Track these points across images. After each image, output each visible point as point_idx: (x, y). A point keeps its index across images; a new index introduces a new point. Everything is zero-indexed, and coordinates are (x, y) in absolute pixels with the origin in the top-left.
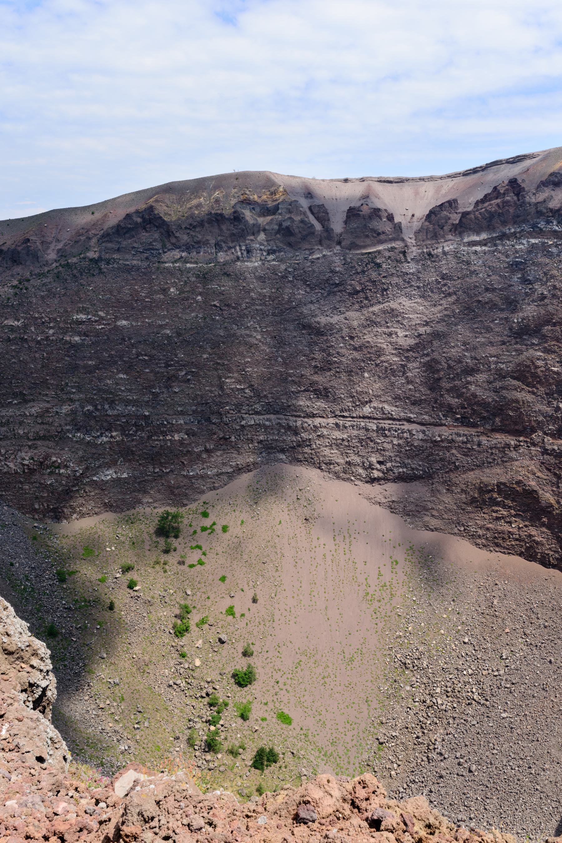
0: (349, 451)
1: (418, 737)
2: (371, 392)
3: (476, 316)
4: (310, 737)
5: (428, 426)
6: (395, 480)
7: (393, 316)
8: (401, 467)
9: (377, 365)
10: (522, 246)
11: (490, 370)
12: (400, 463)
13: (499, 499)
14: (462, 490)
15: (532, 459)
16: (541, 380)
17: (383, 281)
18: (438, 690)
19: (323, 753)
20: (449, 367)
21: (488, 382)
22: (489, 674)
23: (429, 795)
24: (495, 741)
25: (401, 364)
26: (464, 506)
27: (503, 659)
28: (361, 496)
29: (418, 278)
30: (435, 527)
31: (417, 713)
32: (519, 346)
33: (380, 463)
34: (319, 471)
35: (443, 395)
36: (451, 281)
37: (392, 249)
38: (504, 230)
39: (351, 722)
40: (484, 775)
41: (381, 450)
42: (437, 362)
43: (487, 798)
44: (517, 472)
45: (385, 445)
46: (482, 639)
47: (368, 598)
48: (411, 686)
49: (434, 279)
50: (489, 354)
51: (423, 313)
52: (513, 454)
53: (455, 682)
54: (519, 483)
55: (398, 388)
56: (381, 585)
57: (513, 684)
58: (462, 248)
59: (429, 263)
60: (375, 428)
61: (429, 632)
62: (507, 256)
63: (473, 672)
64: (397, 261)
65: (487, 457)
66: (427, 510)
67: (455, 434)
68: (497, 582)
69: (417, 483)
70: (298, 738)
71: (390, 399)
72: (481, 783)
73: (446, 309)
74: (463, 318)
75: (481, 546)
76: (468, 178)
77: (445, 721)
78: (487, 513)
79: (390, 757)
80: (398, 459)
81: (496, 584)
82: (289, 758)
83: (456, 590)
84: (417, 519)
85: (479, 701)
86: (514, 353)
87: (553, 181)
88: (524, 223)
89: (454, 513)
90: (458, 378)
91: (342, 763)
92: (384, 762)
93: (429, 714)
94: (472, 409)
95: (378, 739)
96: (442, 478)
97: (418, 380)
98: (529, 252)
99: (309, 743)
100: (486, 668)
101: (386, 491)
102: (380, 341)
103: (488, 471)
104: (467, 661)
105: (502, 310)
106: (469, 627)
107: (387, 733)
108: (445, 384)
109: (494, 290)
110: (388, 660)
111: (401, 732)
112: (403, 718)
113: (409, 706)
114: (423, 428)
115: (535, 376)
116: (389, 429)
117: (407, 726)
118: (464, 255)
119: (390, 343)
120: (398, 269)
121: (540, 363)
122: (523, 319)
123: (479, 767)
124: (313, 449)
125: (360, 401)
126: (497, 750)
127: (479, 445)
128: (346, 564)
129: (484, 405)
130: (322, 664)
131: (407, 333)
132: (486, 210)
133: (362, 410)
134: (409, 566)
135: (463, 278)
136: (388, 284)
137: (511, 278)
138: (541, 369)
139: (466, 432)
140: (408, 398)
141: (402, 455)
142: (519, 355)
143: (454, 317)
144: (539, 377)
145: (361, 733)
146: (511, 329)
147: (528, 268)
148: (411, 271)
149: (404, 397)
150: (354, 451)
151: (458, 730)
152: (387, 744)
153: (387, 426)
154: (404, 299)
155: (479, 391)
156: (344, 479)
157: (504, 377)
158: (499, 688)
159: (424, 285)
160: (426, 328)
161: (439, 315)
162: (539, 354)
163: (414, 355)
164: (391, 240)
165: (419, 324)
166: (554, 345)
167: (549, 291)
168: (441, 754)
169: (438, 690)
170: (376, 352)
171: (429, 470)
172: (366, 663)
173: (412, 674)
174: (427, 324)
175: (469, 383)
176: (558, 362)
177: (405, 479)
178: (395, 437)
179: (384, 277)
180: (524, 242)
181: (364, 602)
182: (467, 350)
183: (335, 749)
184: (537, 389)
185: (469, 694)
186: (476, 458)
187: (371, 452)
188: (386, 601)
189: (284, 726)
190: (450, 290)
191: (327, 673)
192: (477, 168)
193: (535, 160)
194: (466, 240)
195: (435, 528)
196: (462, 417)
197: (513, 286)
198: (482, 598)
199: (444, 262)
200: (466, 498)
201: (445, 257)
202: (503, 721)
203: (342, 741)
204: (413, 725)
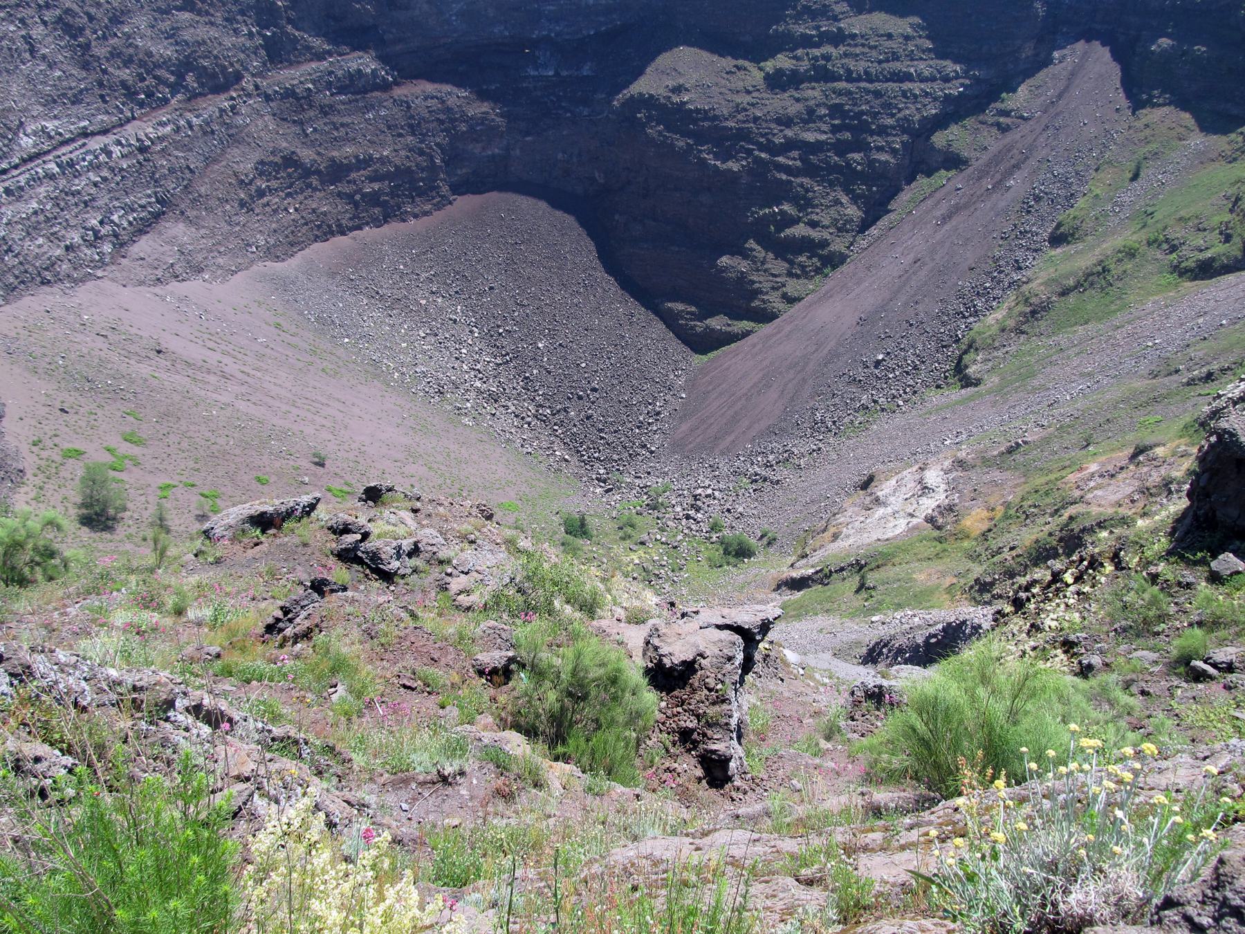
0: (55, 229)
5: (115, 131)
8: (126, 213)
12: (123, 209)
13: (263, 186)
15: (262, 116)
25: (23, 37)
28: (129, 288)
33: (101, 222)
34: (46, 288)
52: (239, 121)
60: (58, 169)
66: (212, 251)
80: (117, 204)
94: (155, 77)
108: (100, 51)
124: (19, 254)
125: (10, 129)
129: (166, 63)
133: (20, 145)
140: (64, 95)
149: (58, 96)
150: (60, 224)
153: (72, 156)
156: (82, 280)
178: (88, 171)
184: (212, 15)
186: (200, 147)
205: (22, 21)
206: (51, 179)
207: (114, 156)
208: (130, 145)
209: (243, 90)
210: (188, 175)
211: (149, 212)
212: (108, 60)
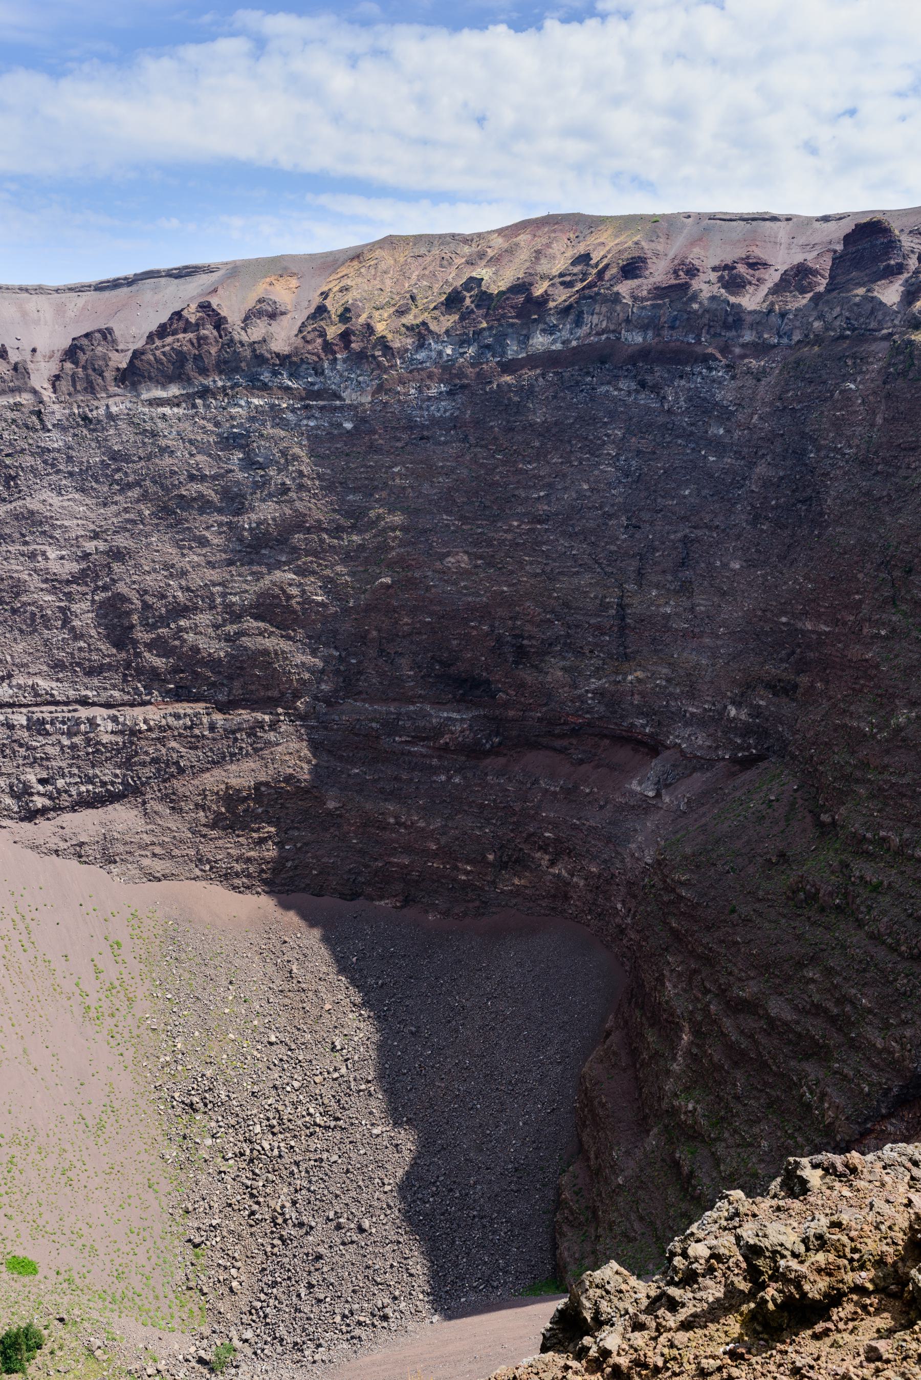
1: (253, 1213)
2: (9, 658)
3: (179, 522)
4: (78, 1281)
5: (120, 708)
6: (73, 807)
7: (34, 524)
8: (82, 783)
9: (14, 611)
10: (240, 410)
11: (215, 607)
12: (80, 777)
14: (197, 805)
15: (302, 740)
16: (299, 616)
17: (7, 462)
18: (258, 1129)
19: (109, 1299)
20: (146, 606)
21: (213, 626)
22: (324, 1079)
23: (310, 1293)
24: (381, 1173)
25: (59, 607)
26: (205, 830)
27: (338, 1051)
29: (68, 457)
30: (162, 873)
31: (238, 1176)
32: (255, 568)
33: (42, 781)
35: (141, 653)
36: (127, 463)
37: (17, 407)
38: (206, 382)
39: (136, 1231)
40: (387, 1227)
41: (42, 758)
42: (124, 599)
43: (406, 1259)
44: (283, 762)
45: (50, 750)
46: (295, 1030)
47: (91, 1015)
48: (213, 1137)
49: (97, 459)
50: (210, 581)
51: (87, 518)
52: (272, 736)
53: (280, 1108)
54: (289, 779)
55: (58, 649)
56: (105, 987)
57: (369, 1082)
58: (141, 409)
59: (85, 432)
60: (25, 723)
61: (211, 1043)
62: (217, 424)
63: (300, 1084)
64: (28, 428)
65: (229, 746)
67: (171, 715)
68: (287, 939)
69: (117, 806)
70: (59, 1290)
71: (45, 668)
72: (387, 1241)
73: (126, 510)
74: (157, 525)
75: (242, 889)
76: (107, 294)
77: (285, 1173)
78: (243, 836)
79: (220, 1262)
81: (285, 942)
82: (59, 1331)
83: (229, 966)
84: (129, 866)
85: (327, 1124)
86: (249, 578)
87: (266, 311)
88: (237, 373)
89: (190, 845)
90: (162, 623)
91: (145, 1302)
92: (213, 1272)
93: (257, 1171)
95: (190, 1241)
96: (160, 790)
97: (93, 632)
98: (252, 419)
99: (79, 1292)
100: (318, 1072)
101: (62, 828)
102: (15, 567)
103: (233, 767)
104: (284, 1070)
105: (220, 511)
106: (269, 1017)
107: (201, 1226)
108: (142, 635)
109: (203, 478)
110: (162, 1107)
111: (222, 1216)
112: (218, 1192)
113: (222, 1169)
114: (113, 712)
115: (289, 610)
116: (52, 720)
117: (229, 1201)
118: (145, 421)
119: (35, 571)
120: (31, 441)
121: (294, 591)
122: (259, 523)
123: (374, 1220)
126: (389, 1184)
127: (212, 727)
128: (33, 968)
129: (213, 663)
130: (53, 1150)
131: (64, 553)
132: (173, 349)
134: (141, 946)
135: (149, 458)
136: (17, 467)
137: (229, 459)
138: (298, 600)
139: (189, 711)
140: (79, 664)
141: (81, 763)
142: (258, 580)
143: (143, 524)
144: (295, 612)
145: (159, 1241)
146: (241, 540)
147: (255, 444)
148: (56, 445)
149: (71, 664)
151: (314, 1179)
152: (208, 1243)
153: (48, 717)
154: (49, 493)
155: (201, 641)
157: (240, 617)
158: (350, 1095)
159: (81, 469)
160: (95, 543)
161: (115, 520)
162: (292, 576)
163: (79, 588)
164: (12, 391)
165: (82, 536)
166: (311, 562)
167: (294, 479)
168: (301, 1225)
169: (258, 1129)
170: (12, 587)
171: (134, 781)
172: (126, 1124)
173: (207, 1118)
174: (96, 536)
175: (180, 629)
176: (320, 587)
177: (93, 803)
178: (63, 734)
179: (7, 455)
180: (243, 403)
181: (87, 1023)
182: (171, 575)
183: (126, 1284)
185: (307, 1119)
187: (24, 765)
188: (124, 1013)
189: (26, 1280)
190: (130, 479)
191: (67, 1161)
192: (119, 279)
193: (214, 276)
194: (145, 396)
195: (163, 875)
196: (177, 687)
197: (233, 471)
198: (270, 969)
199: (112, 432)
200: (207, 817)
201: (112, 423)
202: (379, 1140)
203: (134, 1266)
204: (239, 1197)
205: (69, 596)
206: (8, 728)
207: (102, 728)
208: (124, 724)
209: (296, 709)
210: (173, 769)
211: (107, 790)
212: (146, 645)
